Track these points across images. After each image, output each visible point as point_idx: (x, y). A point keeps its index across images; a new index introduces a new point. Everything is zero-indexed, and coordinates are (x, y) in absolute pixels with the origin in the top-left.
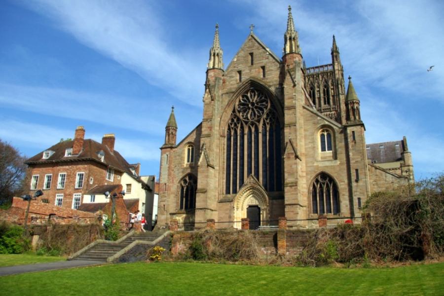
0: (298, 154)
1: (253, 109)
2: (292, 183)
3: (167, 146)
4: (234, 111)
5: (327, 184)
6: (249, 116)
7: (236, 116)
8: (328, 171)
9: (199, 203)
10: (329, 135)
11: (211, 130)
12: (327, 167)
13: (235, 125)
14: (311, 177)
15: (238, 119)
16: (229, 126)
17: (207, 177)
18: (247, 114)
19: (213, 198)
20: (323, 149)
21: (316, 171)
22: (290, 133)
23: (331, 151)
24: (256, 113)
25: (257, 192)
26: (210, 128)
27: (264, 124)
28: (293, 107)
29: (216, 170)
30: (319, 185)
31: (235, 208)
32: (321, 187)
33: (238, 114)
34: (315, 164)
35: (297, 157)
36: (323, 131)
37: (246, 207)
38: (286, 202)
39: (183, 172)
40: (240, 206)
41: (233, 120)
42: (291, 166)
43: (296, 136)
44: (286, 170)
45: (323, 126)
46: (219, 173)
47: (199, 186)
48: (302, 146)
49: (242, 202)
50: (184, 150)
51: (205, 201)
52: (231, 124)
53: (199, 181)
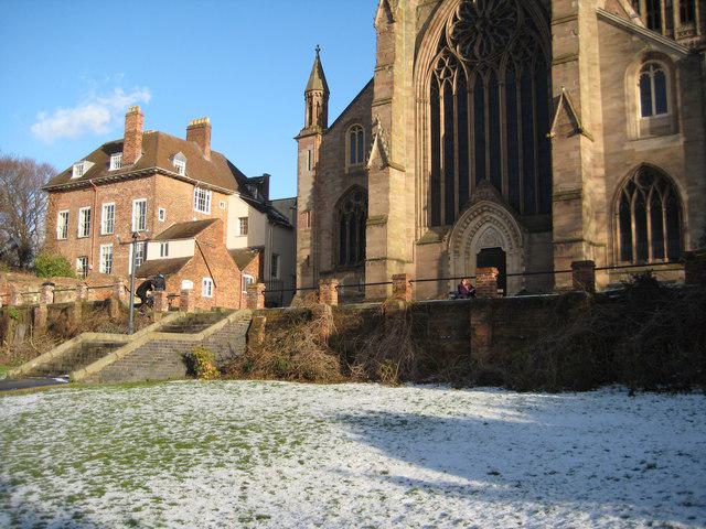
0: (586, 125)
1: (485, 35)
2: (570, 193)
3: (309, 132)
4: (443, 43)
5: (655, 192)
6: (476, 49)
7: (447, 54)
8: (655, 161)
9: (371, 250)
10: (660, 79)
11: (392, 88)
12: (655, 151)
13: (448, 73)
14: (617, 178)
15: (454, 60)
16: (434, 77)
17: (387, 190)
18: (473, 45)
19: (404, 236)
20: (646, 111)
21: (628, 162)
22: (565, 79)
23: (666, 115)
24: (493, 41)
25: (499, 219)
26: (391, 84)
27: (510, 66)
28: (574, 17)
29: (408, 175)
30: (635, 195)
31: (451, 256)
32: (640, 201)
33: (452, 50)
34: (626, 148)
35: (578, 131)
36: (645, 69)
37: (475, 251)
38: (556, 238)
39: (343, 185)
40: (462, 249)
41: (441, 64)
42: (568, 155)
43: (578, 83)
44: (555, 164)
45: (649, 55)
46: (416, 180)
47: (372, 212)
48: (592, 110)
49: (464, 241)
50: (343, 138)
51: (384, 243)
52: (439, 72)
53: (371, 201)
